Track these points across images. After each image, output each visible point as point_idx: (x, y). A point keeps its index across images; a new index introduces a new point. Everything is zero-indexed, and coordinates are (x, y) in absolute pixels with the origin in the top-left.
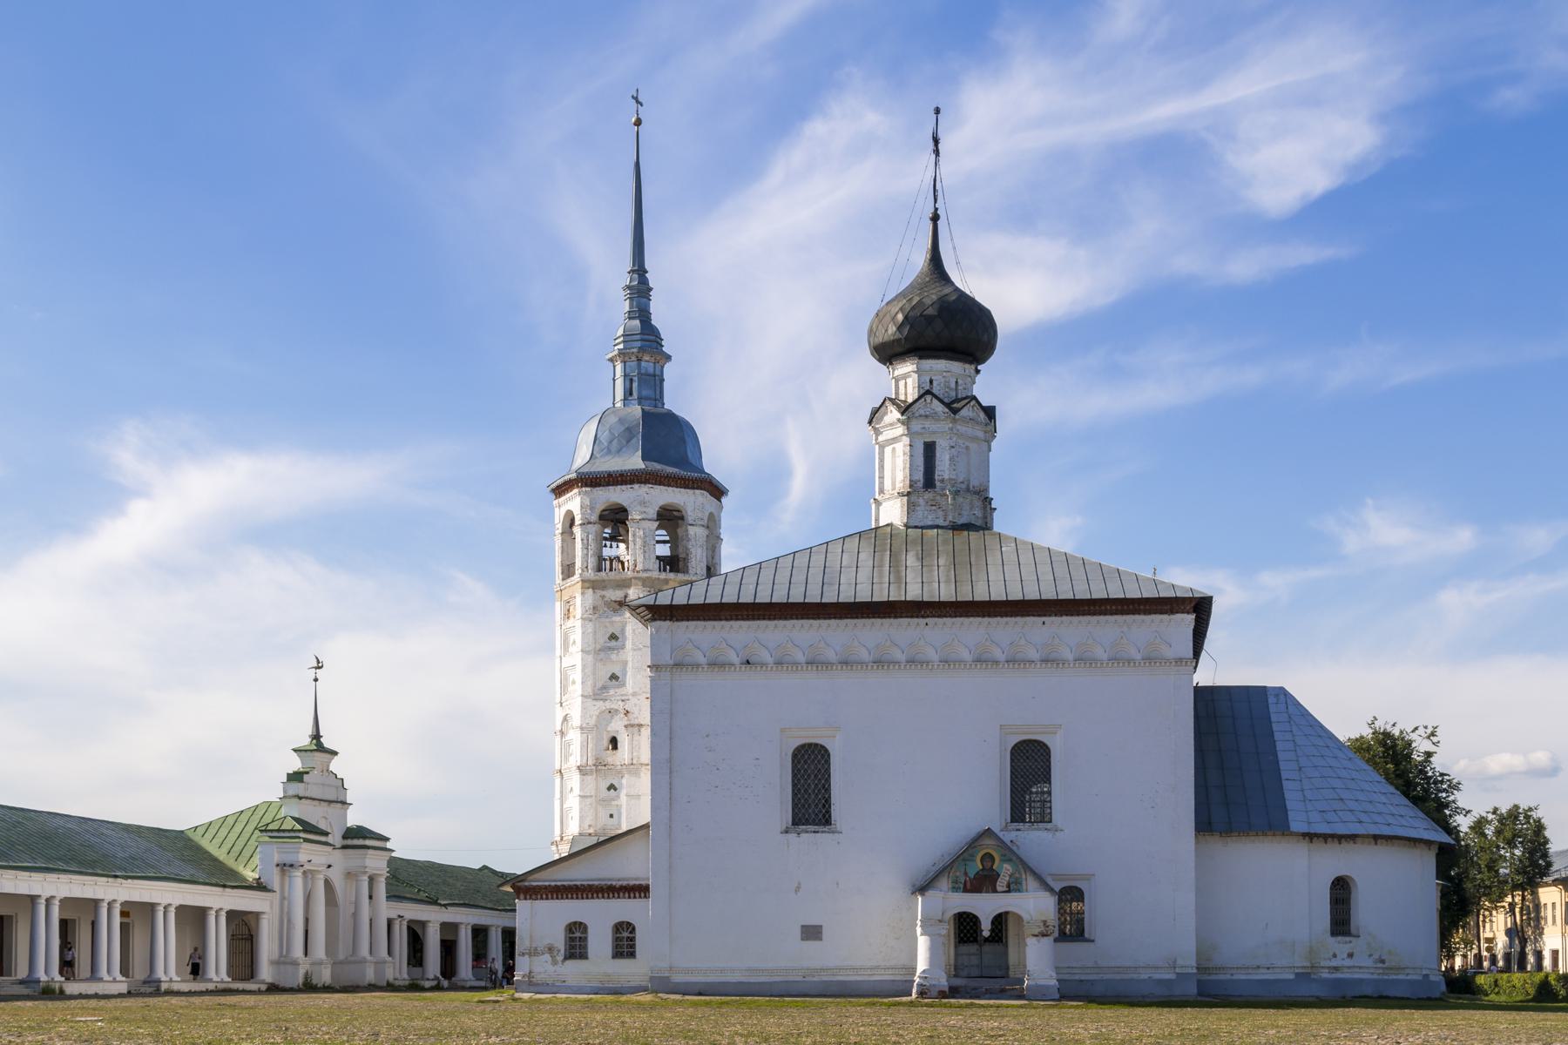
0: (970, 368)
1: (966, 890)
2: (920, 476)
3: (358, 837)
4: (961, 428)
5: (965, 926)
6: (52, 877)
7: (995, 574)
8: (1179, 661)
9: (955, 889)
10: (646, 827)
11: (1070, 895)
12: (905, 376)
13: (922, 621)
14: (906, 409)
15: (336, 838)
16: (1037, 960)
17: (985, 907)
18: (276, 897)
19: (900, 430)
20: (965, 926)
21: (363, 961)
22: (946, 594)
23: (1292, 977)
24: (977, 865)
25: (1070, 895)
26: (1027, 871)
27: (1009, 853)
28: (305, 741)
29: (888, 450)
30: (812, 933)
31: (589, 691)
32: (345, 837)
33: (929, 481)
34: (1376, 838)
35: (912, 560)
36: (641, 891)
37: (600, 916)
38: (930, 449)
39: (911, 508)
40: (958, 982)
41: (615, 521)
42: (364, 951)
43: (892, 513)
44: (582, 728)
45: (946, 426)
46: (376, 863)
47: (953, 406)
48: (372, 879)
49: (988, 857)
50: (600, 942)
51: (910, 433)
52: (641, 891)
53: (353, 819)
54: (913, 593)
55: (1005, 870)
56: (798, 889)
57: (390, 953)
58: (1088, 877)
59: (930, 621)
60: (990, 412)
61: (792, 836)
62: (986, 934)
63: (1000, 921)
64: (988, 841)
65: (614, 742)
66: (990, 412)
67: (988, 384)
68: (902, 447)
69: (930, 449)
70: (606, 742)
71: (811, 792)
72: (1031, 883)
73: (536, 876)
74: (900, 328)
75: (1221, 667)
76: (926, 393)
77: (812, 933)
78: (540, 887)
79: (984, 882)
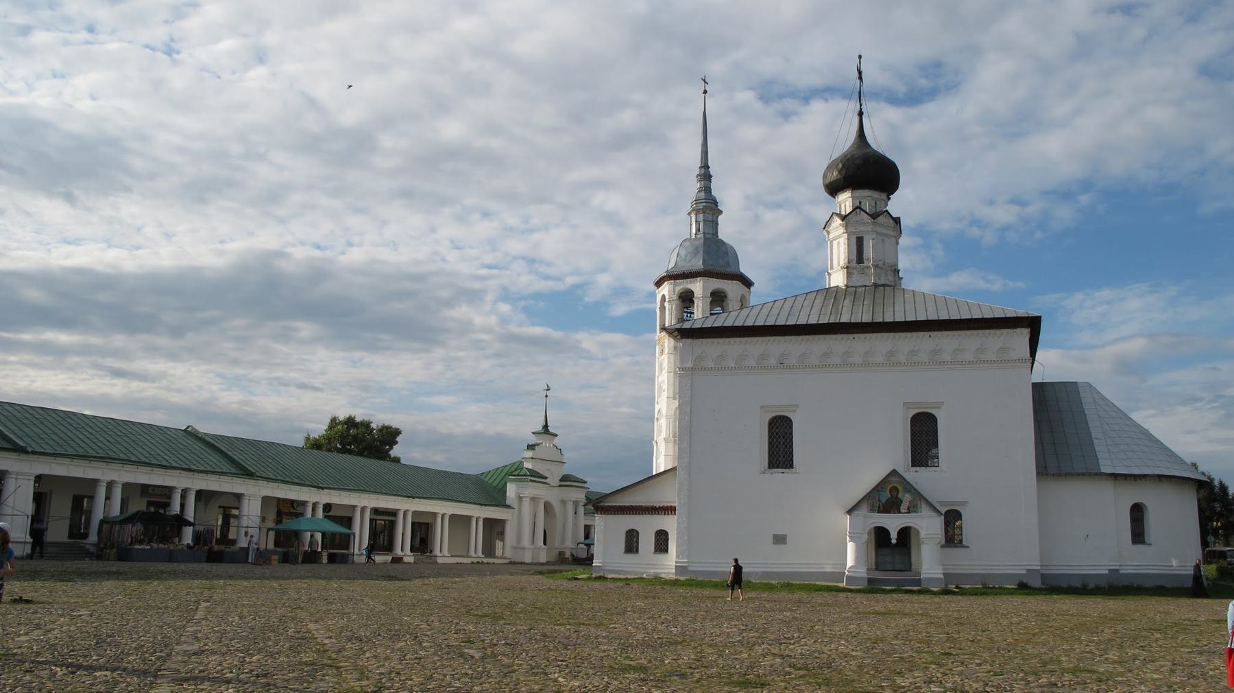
0: (884, 196)
2: (854, 257)
3: (567, 480)
4: (879, 229)
5: (881, 535)
6: (364, 495)
7: (899, 307)
8: (1021, 360)
9: (872, 511)
10: (674, 469)
11: (952, 518)
12: (844, 201)
13: (851, 336)
14: (843, 218)
15: (554, 480)
16: (930, 561)
17: (893, 523)
18: (516, 511)
19: (842, 230)
20: (881, 535)
21: (524, 549)
22: (867, 318)
24: (889, 495)
25: (952, 518)
26: (919, 500)
27: (909, 488)
28: (539, 428)
29: (835, 243)
30: (780, 539)
32: (561, 480)
33: (860, 259)
34: (1160, 478)
35: (847, 303)
36: (670, 510)
37: (647, 527)
38: (860, 242)
39: (849, 275)
40: (878, 575)
41: (686, 299)
42: (526, 542)
43: (838, 279)
45: (870, 228)
46: (580, 496)
47: (875, 216)
48: (576, 503)
50: (647, 542)
52: (670, 510)
53: (566, 470)
54: (845, 319)
55: (906, 498)
57: (545, 543)
58: (964, 503)
59: (856, 336)
60: (897, 221)
61: (768, 476)
62: (894, 541)
63: (905, 533)
64: (894, 479)
66: (897, 221)
67: (897, 204)
68: (843, 240)
69: (860, 242)
71: (780, 445)
73: (617, 496)
75: (1052, 363)
76: (857, 208)
77: (780, 539)
79: (891, 506)
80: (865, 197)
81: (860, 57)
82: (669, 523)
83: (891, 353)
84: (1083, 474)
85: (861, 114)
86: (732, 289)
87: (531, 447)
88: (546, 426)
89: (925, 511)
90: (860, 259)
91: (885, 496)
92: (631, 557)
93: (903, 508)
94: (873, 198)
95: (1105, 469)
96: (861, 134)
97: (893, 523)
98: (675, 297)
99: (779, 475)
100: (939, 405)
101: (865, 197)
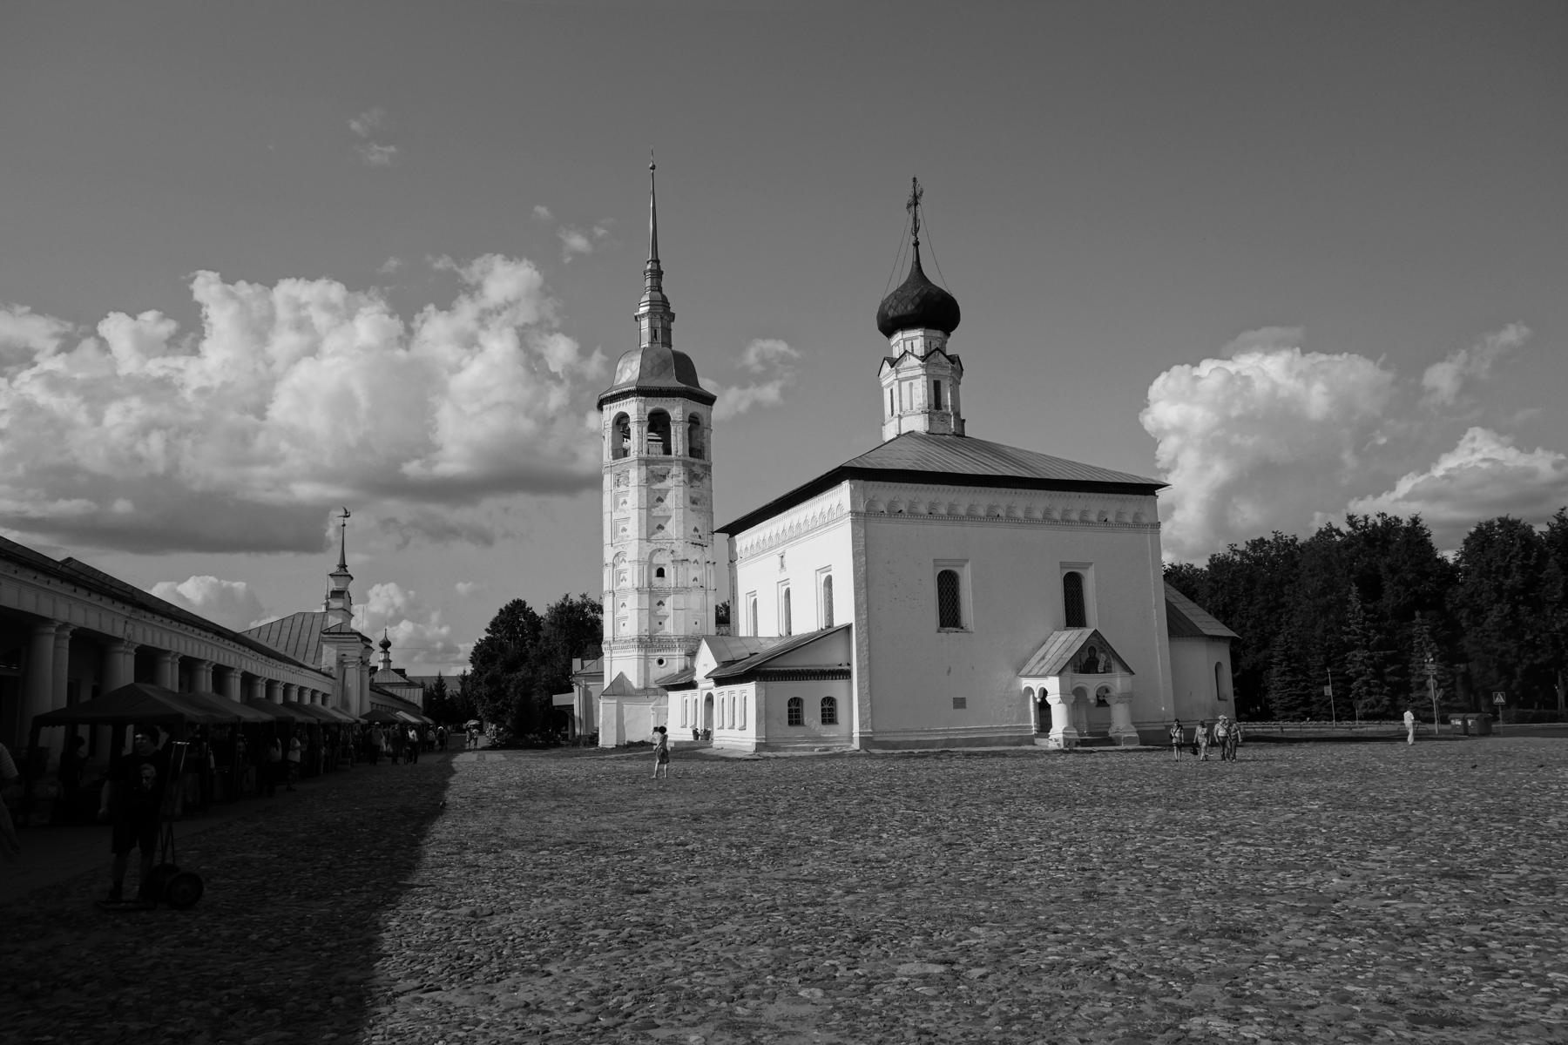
14: (923, 359)
28: (334, 569)
30: (960, 703)
31: (644, 536)
37: (812, 693)
38: (937, 385)
49: (1092, 649)
50: (812, 714)
51: (928, 375)
55: (1102, 657)
65: (661, 573)
69: (937, 385)
70: (654, 572)
72: (1116, 666)
74: (917, 307)
77: (960, 703)
82: (834, 688)
85: (916, 244)
87: (337, 594)
88: (343, 566)
91: (1085, 656)
95: (1206, 632)
97: (1092, 683)
99: (951, 636)
100: (1087, 566)
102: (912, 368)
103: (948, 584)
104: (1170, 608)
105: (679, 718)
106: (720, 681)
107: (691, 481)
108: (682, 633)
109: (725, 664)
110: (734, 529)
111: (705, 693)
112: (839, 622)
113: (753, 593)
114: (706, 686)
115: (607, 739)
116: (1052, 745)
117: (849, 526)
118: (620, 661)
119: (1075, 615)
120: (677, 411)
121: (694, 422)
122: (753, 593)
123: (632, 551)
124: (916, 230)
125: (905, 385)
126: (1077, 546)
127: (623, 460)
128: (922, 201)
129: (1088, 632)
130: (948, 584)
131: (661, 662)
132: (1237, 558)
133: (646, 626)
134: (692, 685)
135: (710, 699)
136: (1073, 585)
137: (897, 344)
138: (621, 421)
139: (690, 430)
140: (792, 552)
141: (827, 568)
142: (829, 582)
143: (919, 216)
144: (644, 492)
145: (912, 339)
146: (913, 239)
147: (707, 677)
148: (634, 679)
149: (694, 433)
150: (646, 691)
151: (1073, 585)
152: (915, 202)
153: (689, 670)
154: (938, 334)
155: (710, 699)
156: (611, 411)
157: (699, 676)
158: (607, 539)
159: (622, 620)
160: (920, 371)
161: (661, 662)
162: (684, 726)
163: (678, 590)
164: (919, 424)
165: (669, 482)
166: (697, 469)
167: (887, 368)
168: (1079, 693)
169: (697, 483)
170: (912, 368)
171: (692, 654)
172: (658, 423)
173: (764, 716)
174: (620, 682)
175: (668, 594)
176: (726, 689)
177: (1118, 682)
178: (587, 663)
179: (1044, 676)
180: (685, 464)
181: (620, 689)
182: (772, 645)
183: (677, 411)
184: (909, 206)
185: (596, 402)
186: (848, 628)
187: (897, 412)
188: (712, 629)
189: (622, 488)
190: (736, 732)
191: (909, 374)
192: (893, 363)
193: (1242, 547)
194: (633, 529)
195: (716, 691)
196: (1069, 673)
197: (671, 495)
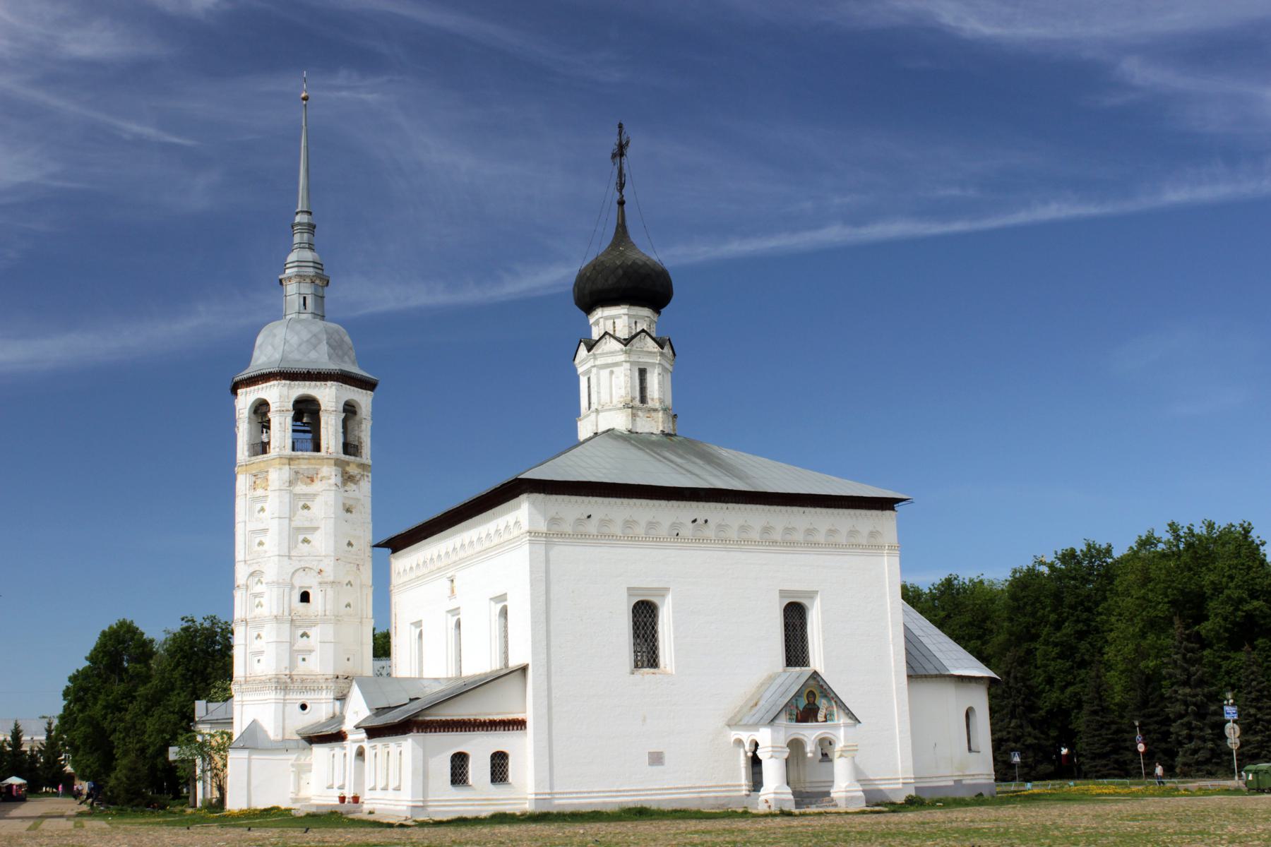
1: (798, 721)
2: (637, 395)
9: (791, 720)
12: (619, 317)
14: (626, 342)
23: (952, 783)
27: (827, 692)
31: (285, 551)
37: (479, 747)
38: (642, 372)
44: (278, 583)
49: (811, 694)
50: (479, 769)
55: (823, 704)
56: (644, 720)
65: (305, 597)
69: (642, 372)
70: (297, 597)
77: (656, 758)
78: (432, 722)
79: (808, 714)
80: (643, 317)
81: (620, 126)
83: (809, 532)
84: (936, 676)
85: (621, 203)
86: (364, 399)
89: (841, 719)
90: (643, 399)
91: (803, 703)
92: (458, 793)
93: (821, 717)
94: (629, 316)
96: (622, 230)
97: (810, 734)
98: (290, 407)
101: (643, 317)
102: (612, 353)
103: (644, 616)
104: (911, 641)
105: (318, 781)
106: (374, 732)
107: (344, 483)
108: (330, 672)
109: (379, 711)
110: (398, 543)
111: (356, 745)
112: (514, 662)
113: (418, 624)
114: (356, 738)
115: (235, 802)
116: (762, 808)
117: (526, 548)
118: (252, 706)
119: (796, 651)
120: (328, 396)
121: (350, 410)
122: (418, 624)
123: (271, 570)
124: (621, 186)
125: (605, 373)
126: (795, 570)
127: (261, 457)
128: (629, 152)
129: (807, 671)
130: (644, 616)
131: (304, 707)
132: (1045, 570)
133: (286, 663)
134: (339, 737)
135: (360, 754)
136: (795, 616)
137: (597, 323)
138: (261, 408)
139: (345, 422)
140: (461, 577)
141: (502, 598)
142: (504, 613)
143: (625, 171)
144: (286, 498)
145: (613, 318)
146: (617, 196)
147: (357, 727)
148: (272, 730)
149: (350, 424)
150: (282, 747)
151: (795, 616)
152: (621, 151)
153: (338, 718)
154: (646, 312)
155: (360, 754)
156: (246, 399)
157: (348, 726)
158: (239, 555)
159: (253, 655)
160: (622, 358)
161: (304, 707)
162: (330, 787)
163: (324, 620)
164: (620, 421)
165: (317, 487)
166: (352, 470)
167: (583, 350)
168: (796, 746)
169: (351, 486)
170: (612, 353)
171: (342, 698)
172: (306, 411)
173: (424, 775)
174: (254, 728)
175: (314, 624)
176: (379, 743)
177: (841, 733)
178: (212, 706)
179: (756, 726)
180: (338, 463)
181: (254, 741)
182: (437, 688)
183: (328, 396)
184: (614, 156)
185: (229, 385)
186: (524, 669)
187: (594, 407)
188: (367, 663)
189: (260, 492)
190: (390, 794)
191: (610, 360)
192: (591, 346)
193: (1049, 558)
194: (272, 544)
195: (367, 745)
196: (783, 720)
197: (319, 500)
